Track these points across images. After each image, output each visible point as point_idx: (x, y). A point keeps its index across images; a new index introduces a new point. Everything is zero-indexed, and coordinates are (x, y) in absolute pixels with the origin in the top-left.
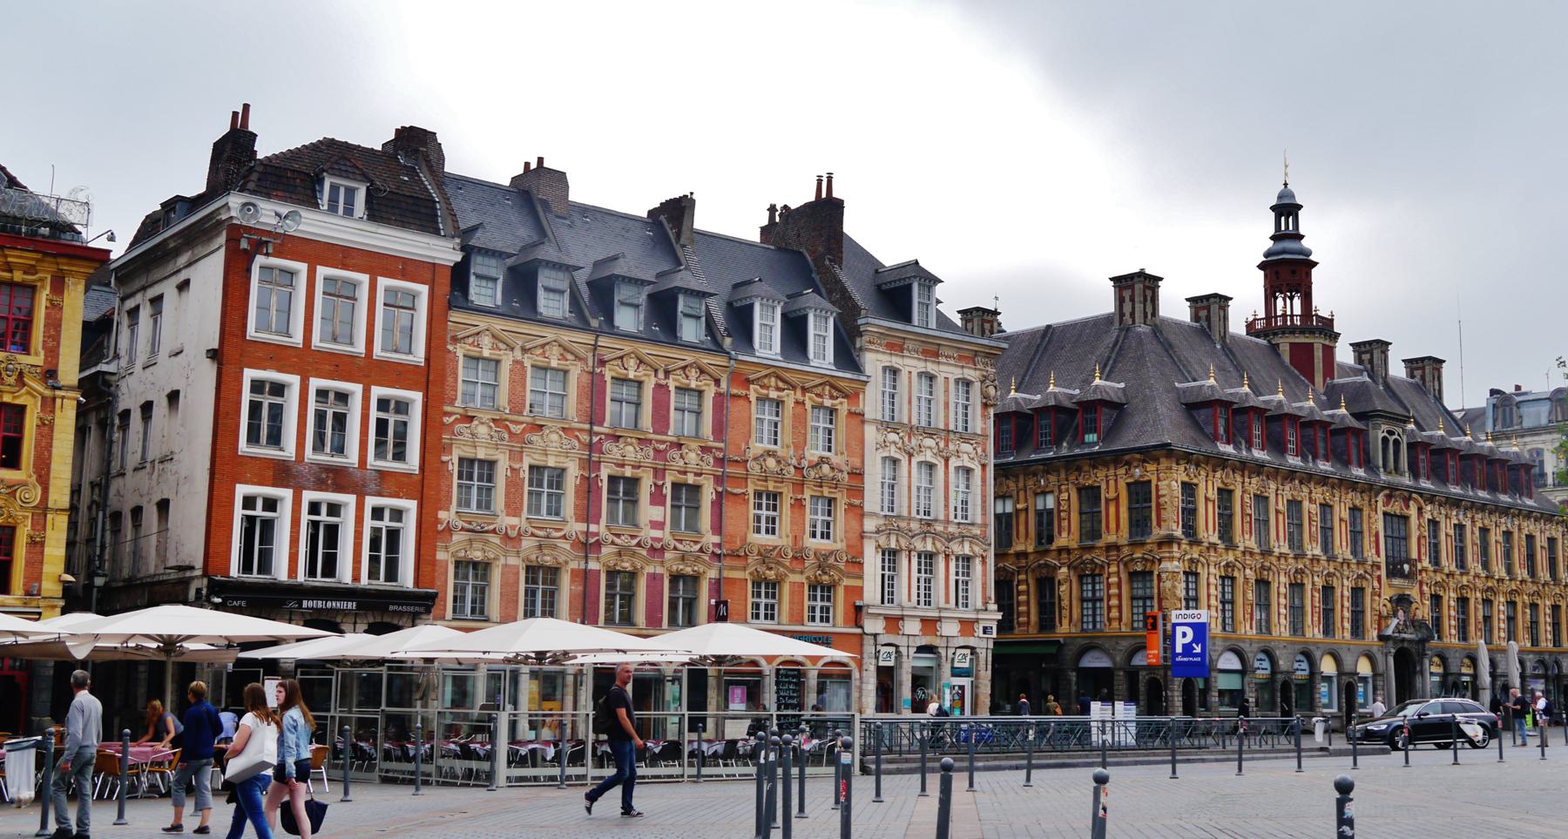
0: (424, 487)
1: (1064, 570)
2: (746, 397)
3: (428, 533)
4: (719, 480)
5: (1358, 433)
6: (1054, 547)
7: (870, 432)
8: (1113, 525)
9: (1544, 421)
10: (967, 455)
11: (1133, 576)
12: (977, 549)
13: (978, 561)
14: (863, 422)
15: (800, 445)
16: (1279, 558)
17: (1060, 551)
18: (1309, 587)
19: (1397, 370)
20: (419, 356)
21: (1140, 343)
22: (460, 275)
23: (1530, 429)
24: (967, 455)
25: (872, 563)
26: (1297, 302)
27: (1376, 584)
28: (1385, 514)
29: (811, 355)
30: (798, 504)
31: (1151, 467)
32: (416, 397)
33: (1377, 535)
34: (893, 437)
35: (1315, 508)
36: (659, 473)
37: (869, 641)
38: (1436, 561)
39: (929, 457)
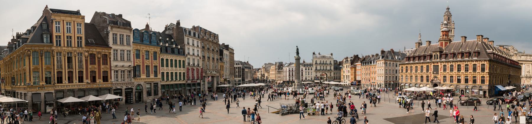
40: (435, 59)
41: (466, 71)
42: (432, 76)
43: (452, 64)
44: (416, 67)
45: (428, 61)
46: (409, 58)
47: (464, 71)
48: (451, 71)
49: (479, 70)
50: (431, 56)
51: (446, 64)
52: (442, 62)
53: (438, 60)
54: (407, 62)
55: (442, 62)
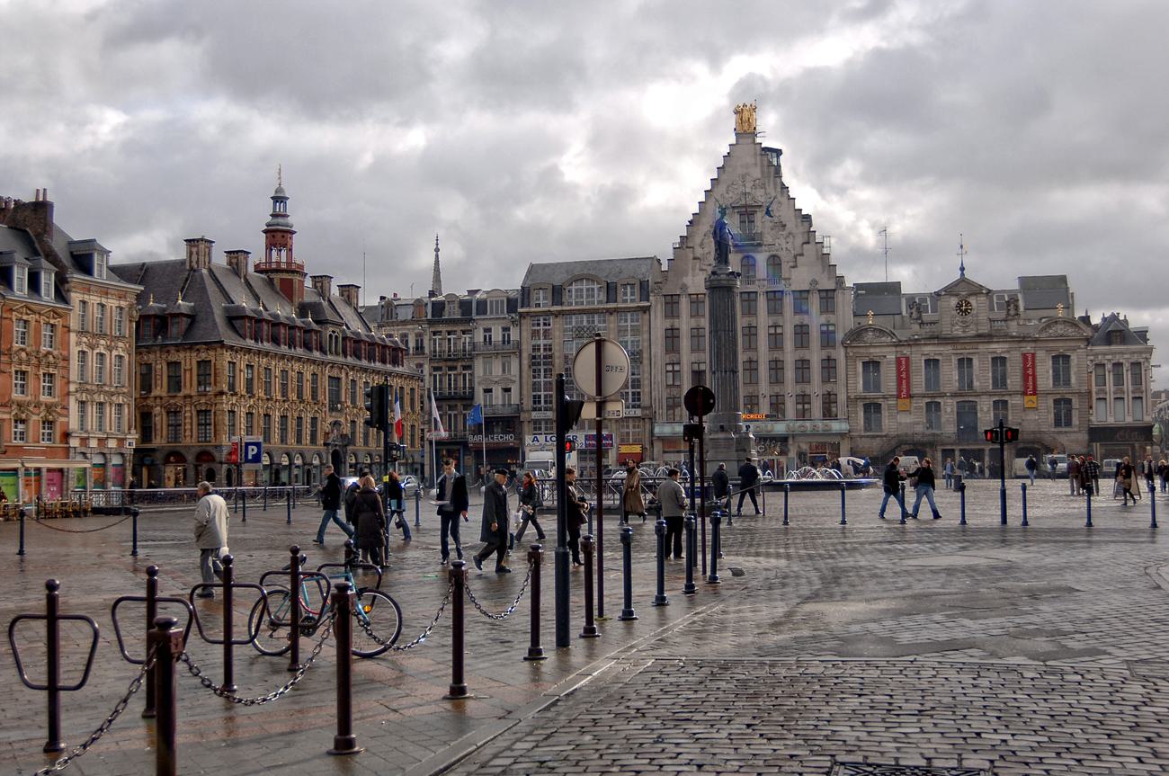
1: (158, 408)
2: (11, 319)
5: (316, 332)
6: (153, 394)
7: (73, 337)
8: (188, 384)
9: (410, 317)
10: (121, 349)
11: (199, 412)
13: (126, 406)
14: (69, 331)
15: (38, 344)
16: (276, 402)
17: (156, 398)
18: (290, 418)
19: (335, 292)
21: (202, 279)
23: (401, 322)
25: (74, 407)
26: (284, 253)
28: (329, 377)
29: (43, 295)
31: (212, 353)
34: (85, 339)
35: (294, 374)
37: (72, 451)
38: (354, 401)
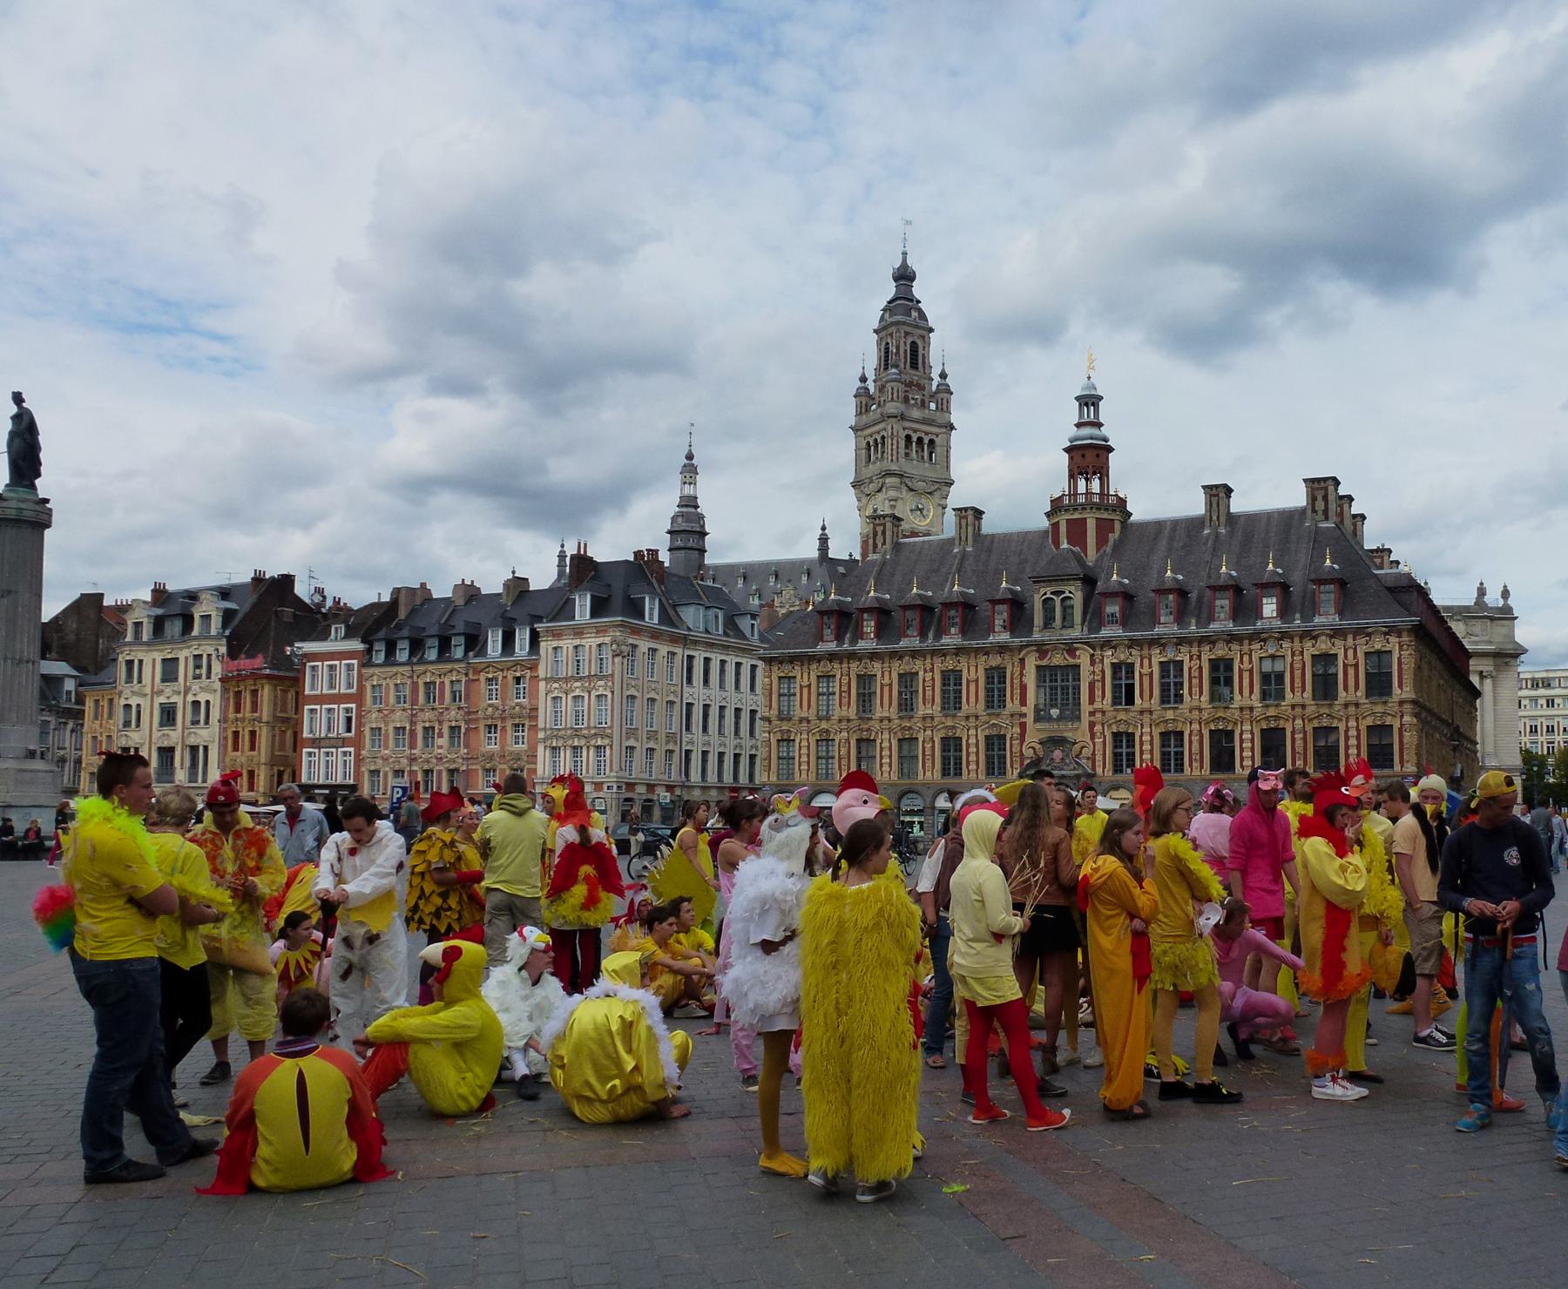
0: (357, 743)
3: (359, 761)
4: (467, 722)
12: (606, 741)
20: (354, 691)
22: (369, 651)
24: (601, 688)
27: (1017, 730)
30: (504, 728)
32: (353, 706)
33: (1023, 688)
36: (440, 723)
39: (577, 693)
40: (1048, 622)
41: (1265, 695)
42: (1033, 737)
43: (1171, 654)
44: (907, 679)
45: (1004, 637)
46: (843, 619)
47: (1255, 700)
48: (1164, 699)
49: (1351, 691)
50: (1018, 609)
51: (1135, 657)
52: (1107, 644)
53: (1075, 633)
54: (832, 646)
55: (1107, 644)
